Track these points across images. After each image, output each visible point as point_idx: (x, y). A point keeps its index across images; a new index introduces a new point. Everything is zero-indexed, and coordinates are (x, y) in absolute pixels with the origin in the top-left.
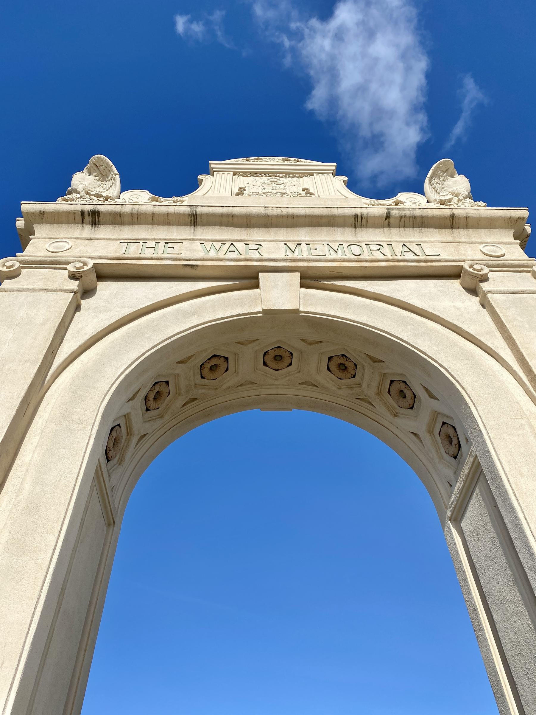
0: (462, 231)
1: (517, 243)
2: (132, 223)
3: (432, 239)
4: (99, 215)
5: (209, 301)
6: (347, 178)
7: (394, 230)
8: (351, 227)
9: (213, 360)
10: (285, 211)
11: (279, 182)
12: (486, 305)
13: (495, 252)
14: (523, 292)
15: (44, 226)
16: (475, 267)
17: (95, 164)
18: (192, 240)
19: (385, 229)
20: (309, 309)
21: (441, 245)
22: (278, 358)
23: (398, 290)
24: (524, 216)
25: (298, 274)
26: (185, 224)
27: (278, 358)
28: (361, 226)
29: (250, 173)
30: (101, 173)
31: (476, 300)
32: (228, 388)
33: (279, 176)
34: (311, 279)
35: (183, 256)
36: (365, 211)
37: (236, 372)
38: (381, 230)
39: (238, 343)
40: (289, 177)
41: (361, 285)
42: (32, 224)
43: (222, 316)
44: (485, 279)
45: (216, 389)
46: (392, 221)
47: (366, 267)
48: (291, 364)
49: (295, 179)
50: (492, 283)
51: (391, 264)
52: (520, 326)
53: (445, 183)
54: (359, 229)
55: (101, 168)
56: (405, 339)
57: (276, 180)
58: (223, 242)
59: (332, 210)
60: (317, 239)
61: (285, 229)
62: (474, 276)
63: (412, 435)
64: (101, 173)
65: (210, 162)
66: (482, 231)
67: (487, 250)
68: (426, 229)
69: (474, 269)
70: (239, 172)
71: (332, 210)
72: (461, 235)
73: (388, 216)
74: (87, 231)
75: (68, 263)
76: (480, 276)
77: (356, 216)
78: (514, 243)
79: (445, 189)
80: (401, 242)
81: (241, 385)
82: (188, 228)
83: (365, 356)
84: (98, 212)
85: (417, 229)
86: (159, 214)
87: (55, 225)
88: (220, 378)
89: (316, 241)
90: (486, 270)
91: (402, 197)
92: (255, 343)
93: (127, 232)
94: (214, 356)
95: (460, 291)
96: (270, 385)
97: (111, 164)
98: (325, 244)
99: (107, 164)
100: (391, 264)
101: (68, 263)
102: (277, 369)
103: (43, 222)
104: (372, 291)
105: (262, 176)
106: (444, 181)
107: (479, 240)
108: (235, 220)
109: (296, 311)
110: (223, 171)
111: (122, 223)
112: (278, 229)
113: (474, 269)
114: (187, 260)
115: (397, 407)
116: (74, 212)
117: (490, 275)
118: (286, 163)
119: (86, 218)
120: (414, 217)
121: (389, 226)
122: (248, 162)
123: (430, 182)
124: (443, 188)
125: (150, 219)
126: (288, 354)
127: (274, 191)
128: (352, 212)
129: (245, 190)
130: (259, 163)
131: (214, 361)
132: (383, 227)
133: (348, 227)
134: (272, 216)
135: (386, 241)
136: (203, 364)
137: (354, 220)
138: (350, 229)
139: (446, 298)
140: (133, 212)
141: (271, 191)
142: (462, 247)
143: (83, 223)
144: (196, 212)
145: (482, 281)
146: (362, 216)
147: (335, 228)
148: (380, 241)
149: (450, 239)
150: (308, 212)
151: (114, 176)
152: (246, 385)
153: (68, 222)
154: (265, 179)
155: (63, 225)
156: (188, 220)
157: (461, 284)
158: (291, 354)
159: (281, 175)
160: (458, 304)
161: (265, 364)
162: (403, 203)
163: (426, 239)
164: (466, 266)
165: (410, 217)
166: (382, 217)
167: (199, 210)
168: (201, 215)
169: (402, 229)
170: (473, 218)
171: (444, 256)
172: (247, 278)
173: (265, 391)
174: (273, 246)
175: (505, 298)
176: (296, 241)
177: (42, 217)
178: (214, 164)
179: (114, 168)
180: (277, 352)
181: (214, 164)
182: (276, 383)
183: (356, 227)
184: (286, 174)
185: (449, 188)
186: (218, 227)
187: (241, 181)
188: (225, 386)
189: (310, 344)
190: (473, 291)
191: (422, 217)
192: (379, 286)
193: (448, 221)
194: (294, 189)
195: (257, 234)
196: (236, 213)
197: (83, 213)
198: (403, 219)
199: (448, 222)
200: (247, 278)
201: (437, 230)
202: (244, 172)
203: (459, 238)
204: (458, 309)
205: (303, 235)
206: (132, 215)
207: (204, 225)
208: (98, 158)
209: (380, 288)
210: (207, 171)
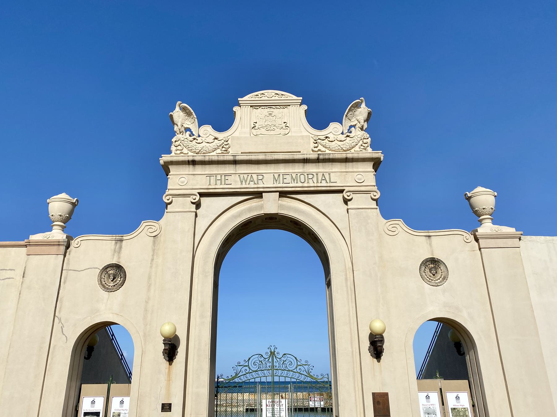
26: (232, 164)
53: (355, 113)
65: (239, 99)
82: (233, 165)
110: (246, 105)
119: (190, 163)
163: (333, 170)
179: (194, 113)
183: (304, 163)
200: (258, 195)
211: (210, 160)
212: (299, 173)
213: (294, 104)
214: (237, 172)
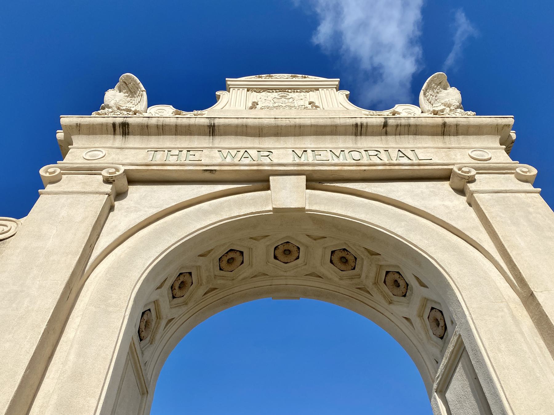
0: (453, 138)
1: (502, 148)
2: (158, 134)
3: (426, 145)
4: (128, 127)
5: (226, 201)
6: (349, 92)
7: (390, 138)
8: (352, 135)
9: (229, 253)
10: (293, 122)
11: (288, 97)
12: (472, 203)
13: (482, 156)
14: (506, 192)
15: (80, 137)
16: (463, 169)
17: (124, 82)
18: (211, 148)
19: (382, 137)
20: (314, 208)
21: (433, 150)
22: (287, 252)
23: (394, 191)
24: (510, 123)
25: (304, 177)
26: (204, 134)
27: (287, 252)
28: (361, 135)
29: (262, 89)
30: (130, 90)
31: (464, 199)
32: (244, 279)
33: (288, 92)
34: (316, 181)
35: (203, 162)
36: (364, 121)
37: (251, 264)
38: (379, 138)
39: (251, 238)
40: (297, 92)
41: (360, 186)
42: (71, 135)
43: (238, 214)
44: (472, 180)
45: (233, 280)
46: (389, 129)
47: (365, 170)
48: (298, 258)
49: (303, 94)
50: (479, 183)
51: (388, 167)
52: (502, 222)
53: (439, 95)
54: (359, 137)
55: (130, 86)
56: (399, 233)
57: (285, 95)
58: (238, 150)
59: (335, 120)
60: (322, 146)
61: (293, 138)
62: (462, 178)
63: (404, 320)
64: (130, 90)
66: (471, 138)
67: (475, 155)
68: (420, 136)
69: (463, 172)
70: (253, 88)
71: (335, 120)
72: (452, 141)
73: (385, 125)
74: (118, 141)
75: (102, 169)
76: (467, 178)
77: (356, 125)
78: (500, 148)
79: (438, 100)
80: (397, 148)
81: (255, 276)
82: (207, 137)
83: (363, 250)
84: (128, 124)
85: (412, 136)
86: (181, 126)
87: (90, 136)
88: (236, 270)
89: (321, 148)
90: (473, 172)
91: (398, 108)
92: (267, 238)
93: (154, 142)
94: (231, 250)
95: (450, 191)
96: (281, 276)
97: (139, 81)
98: (328, 150)
99: (135, 81)
100: (388, 167)
101: (102, 169)
102: (286, 261)
103: (79, 134)
104: (370, 191)
105: (273, 92)
106: (437, 93)
107: (468, 146)
108: (249, 130)
109: (302, 210)
110: (239, 87)
111: (149, 134)
112: (287, 138)
113: (463, 172)
114: (207, 166)
115: (391, 294)
116: (107, 125)
117: (477, 177)
118: (294, 79)
120: (409, 126)
121: (386, 134)
122: (260, 79)
123: (425, 94)
124: (436, 100)
125: (174, 130)
126: (296, 249)
127: (284, 105)
128: (353, 121)
129: (257, 104)
130: (270, 79)
131: (231, 255)
132: (380, 134)
133: (349, 135)
134: (282, 126)
135: (383, 148)
136: (221, 257)
137: (354, 129)
138: (351, 137)
139: (438, 198)
140: (159, 124)
141: (281, 104)
142: (452, 152)
143: (115, 134)
144: (214, 124)
145: (469, 182)
146: (362, 125)
147: (338, 137)
148: (377, 148)
149: (441, 145)
150: (313, 122)
151: (141, 93)
152: (259, 276)
153: (102, 133)
154: (275, 94)
155: (98, 136)
156: (207, 130)
157: (451, 185)
158: (299, 248)
159: (290, 91)
160: (447, 203)
161: (275, 257)
162: (399, 114)
163: (419, 145)
164: (455, 169)
165: (405, 126)
166: (380, 126)
167: (217, 121)
168: (219, 126)
169: (398, 137)
170: (463, 126)
171: (436, 160)
172: (260, 181)
173: (276, 282)
174: (282, 152)
175: (490, 197)
176: (302, 148)
177: (79, 129)
178: (230, 81)
180: (287, 247)
181: (230, 81)
182: (285, 274)
183: (356, 135)
184: (294, 89)
185: (443, 99)
186: (233, 137)
187: (254, 96)
188: (241, 277)
189: (315, 240)
190: (461, 192)
191: (416, 126)
192: (377, 187)
193: (440, 129)
194: (302, 103)
195: (268, 143)
196: (250, 124)
197: (114, 125)
198: (399, 128)
199: (440, 130)
200: (260, 181)
201: (430, 137)
202: (257, 88)
203: (449, 144)
204: (447, 207)
205: (309, 142)
206: (157, 126)
207: (221, 135)
208: (127, 76)
209: (378, 189)
210: (224, 87)
211: (160, 123)
212: (347, 148)
213: (327, 87)
214: (216, 146)
